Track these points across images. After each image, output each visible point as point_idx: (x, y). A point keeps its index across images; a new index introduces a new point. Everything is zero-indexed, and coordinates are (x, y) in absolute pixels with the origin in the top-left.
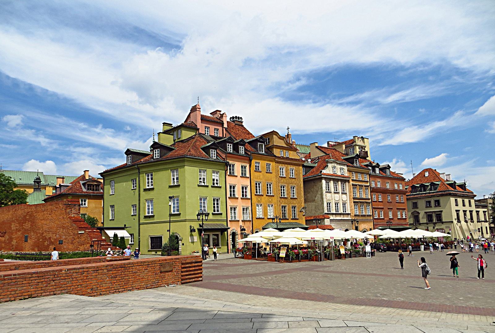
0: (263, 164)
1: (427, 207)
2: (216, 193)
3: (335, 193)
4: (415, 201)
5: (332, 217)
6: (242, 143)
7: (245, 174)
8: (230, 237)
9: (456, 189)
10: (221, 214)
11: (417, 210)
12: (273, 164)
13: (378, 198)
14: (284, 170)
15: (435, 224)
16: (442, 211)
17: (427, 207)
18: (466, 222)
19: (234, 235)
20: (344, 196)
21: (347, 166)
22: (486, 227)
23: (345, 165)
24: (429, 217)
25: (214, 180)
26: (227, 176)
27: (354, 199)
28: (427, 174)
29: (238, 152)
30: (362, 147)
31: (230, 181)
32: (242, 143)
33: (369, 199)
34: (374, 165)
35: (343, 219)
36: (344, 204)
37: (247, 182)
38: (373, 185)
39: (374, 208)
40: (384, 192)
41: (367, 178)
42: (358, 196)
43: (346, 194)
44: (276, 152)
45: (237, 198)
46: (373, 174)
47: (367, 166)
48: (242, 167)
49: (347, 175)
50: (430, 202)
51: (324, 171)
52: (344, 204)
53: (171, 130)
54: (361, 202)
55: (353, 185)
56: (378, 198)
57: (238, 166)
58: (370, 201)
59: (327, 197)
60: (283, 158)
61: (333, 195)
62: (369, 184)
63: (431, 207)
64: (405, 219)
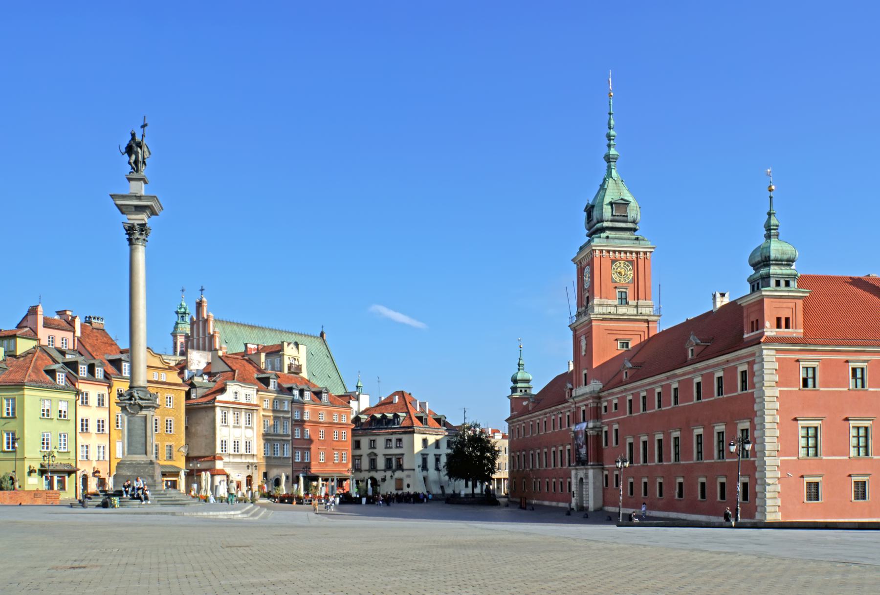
1: (387, 447)
3: (234, 427)
4: (373, 438)
7: (103, 404)
11: (375, 451)
15: (394, 472)
16: (403, 455)
17: (387, 447)
18: (437, 469)
20: (250, 431)
21: (258, 391)
24: (388, 461)
25: (60, 412)
28: (397, 399)
31: (83, 412)
33: (288, 436)
37: (103, 414)
39: (295, 448)
41: (286, 407)
46: (300, 399)
48: (99, 395)
49: (255, 403)
50: (390, 440)
51: (219, 398)
54: (274, 440)
57: (93, 391)
58: (290, 438)
59: (222, 433)
62: (290, 415)
63: (391, 448)
64: (347, 464)
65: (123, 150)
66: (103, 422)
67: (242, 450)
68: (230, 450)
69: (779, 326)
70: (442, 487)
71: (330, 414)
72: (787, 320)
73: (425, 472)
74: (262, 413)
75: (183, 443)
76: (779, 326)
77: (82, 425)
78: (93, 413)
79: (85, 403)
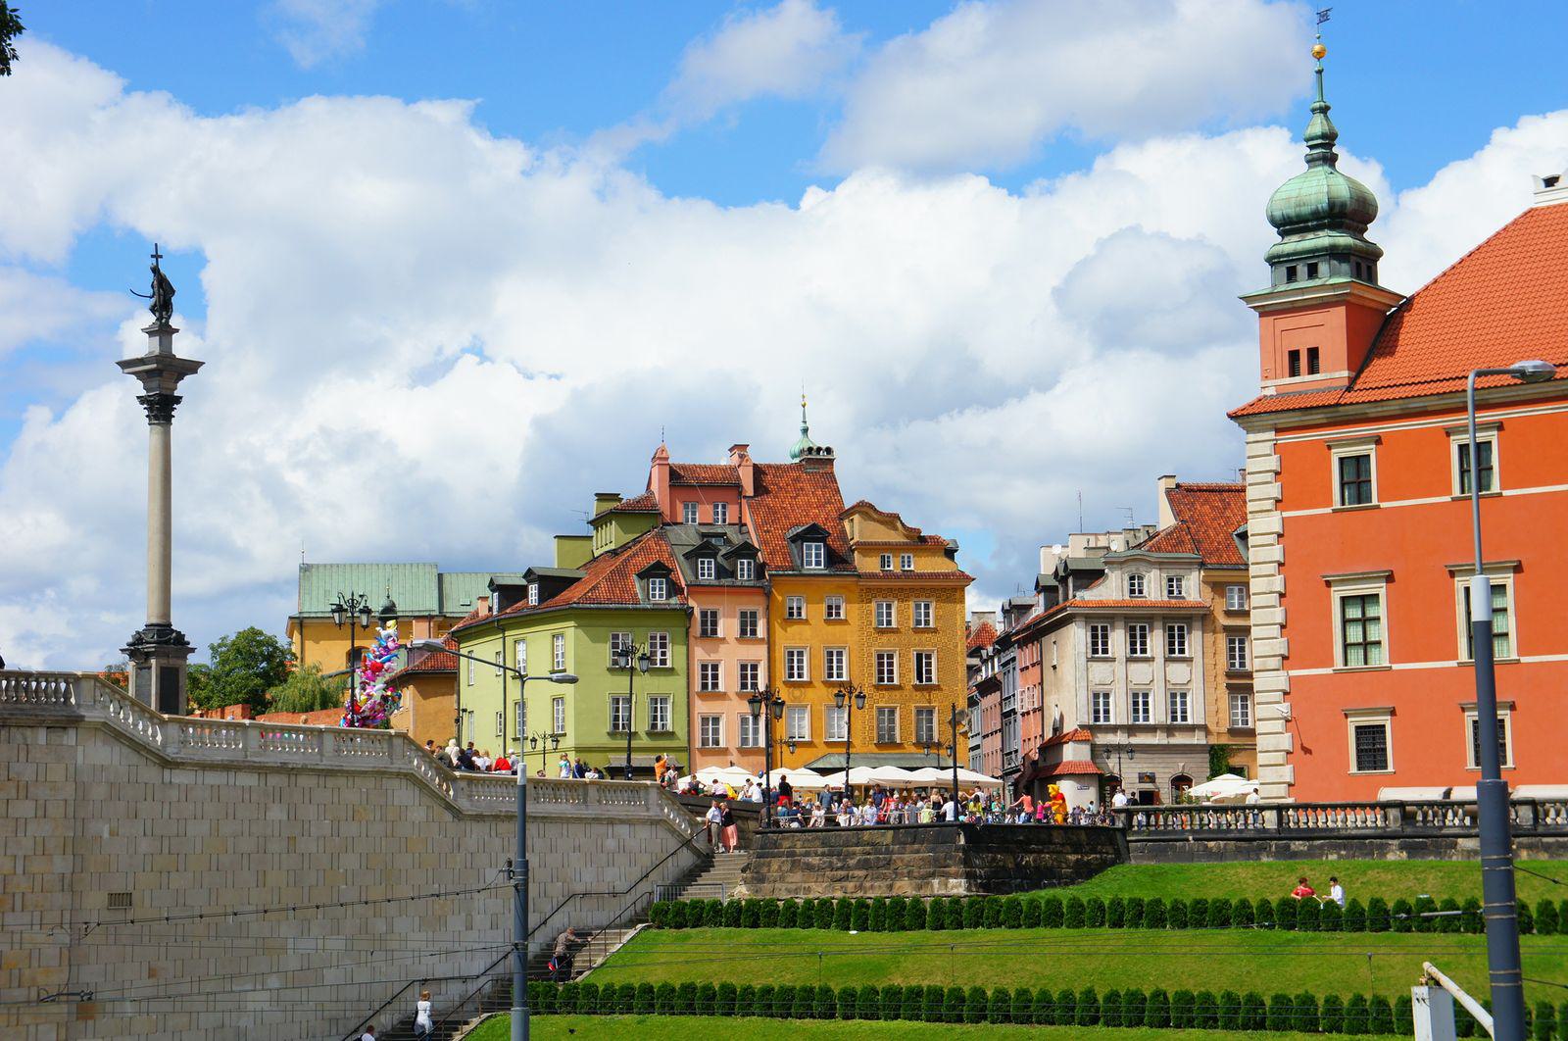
3: (1129, 660)
7: (754, 632)
10: (672, 735)
20: (1182, 667)
21: (1202, 565)
23: (1190, 564)
26: (692, 639)
27: (1229, 675)
29: (733, 574)
35: (1165, 742)
36: (1177, 697)
37: (757, 653)
43: (1190, 660)
44: (867, 564)
45: (723, 696)
48: (743, 615)
53: (614, 510)
55: (1226, 629)
61: (1119, 667)
65: (150, 292)
66: (754, 667)
67: (1158, 714)
68: (1119, 713)
69: (1294, 371)
72: (1313, 353)
74: (1224, 621)
76: (1294, 371)
77: (704, 677)
78: (730, 654)
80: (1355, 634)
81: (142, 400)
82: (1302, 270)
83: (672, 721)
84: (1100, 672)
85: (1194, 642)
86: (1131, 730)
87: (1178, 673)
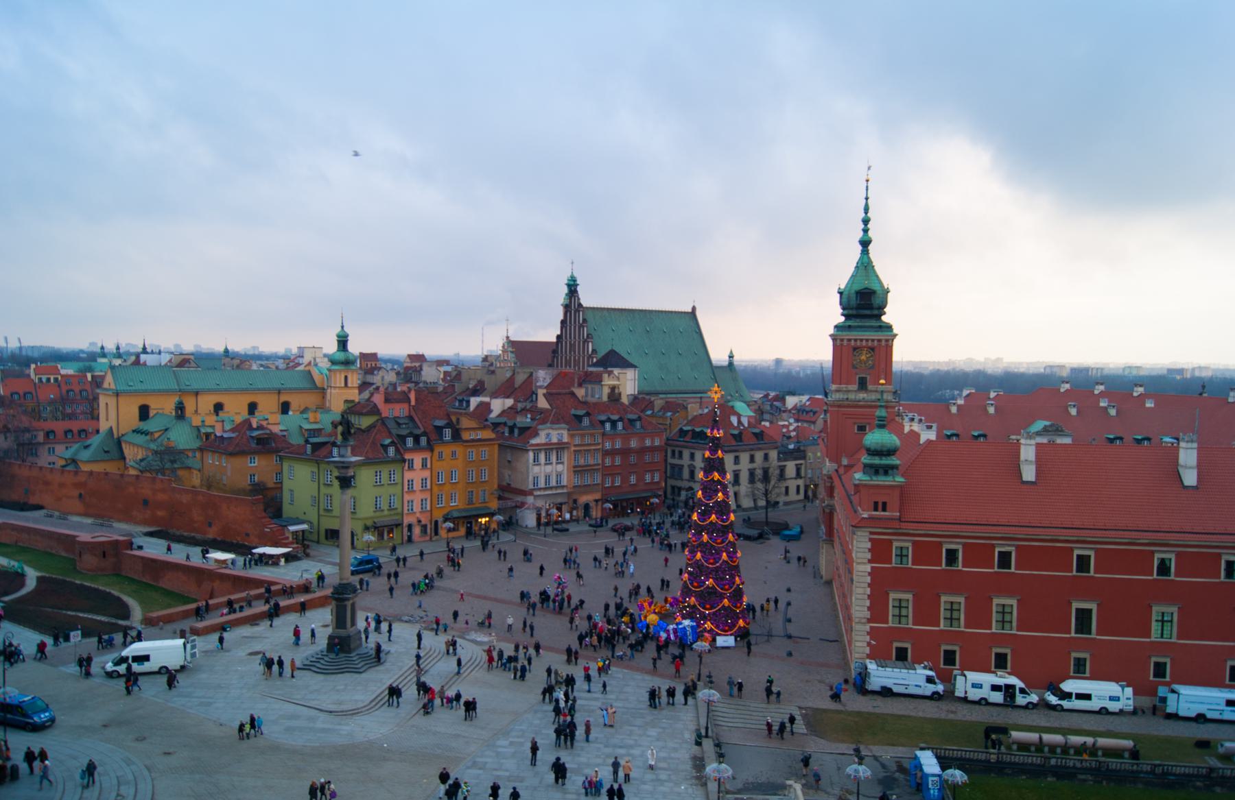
0: (446, 451)
2: (392, 490)
5: (538, 493)
6: (425, 434)
8: (405, 530)
9: (741, 440)
12: (459, 449)
13: (613, 461)
14: (474, 453)
19: (410, 527)
22: (798, 487)
30: (613, 388)
31: (408, 475)
32: (425, 434)
34: (615, 417)
36: (559, 475)
37: (427, 474)
38: (608, 445)
40: (625, 452)
42: (582, 462)
44: (466, 436)
47: (602, 423)
49: (565, 440)
51: (533, 441)
52: (559, 475)
56: (613, 461)
57: (417, 459)
60: (473, 441)
68: (542, 484)
70: (755, 501)
71: (642, 439)
72: (884, 504)
73: (736, 488)
75: (496, 486)
76: (876, 509)
78: (417, 475)
79: (411, 468)
80: (897, 612)
81: (337, 478)
82: (881, 471)
83: (397, 505)
84: (536, 469)
85: (565, 459)
86: (545, 489)
87: (560, 468)
